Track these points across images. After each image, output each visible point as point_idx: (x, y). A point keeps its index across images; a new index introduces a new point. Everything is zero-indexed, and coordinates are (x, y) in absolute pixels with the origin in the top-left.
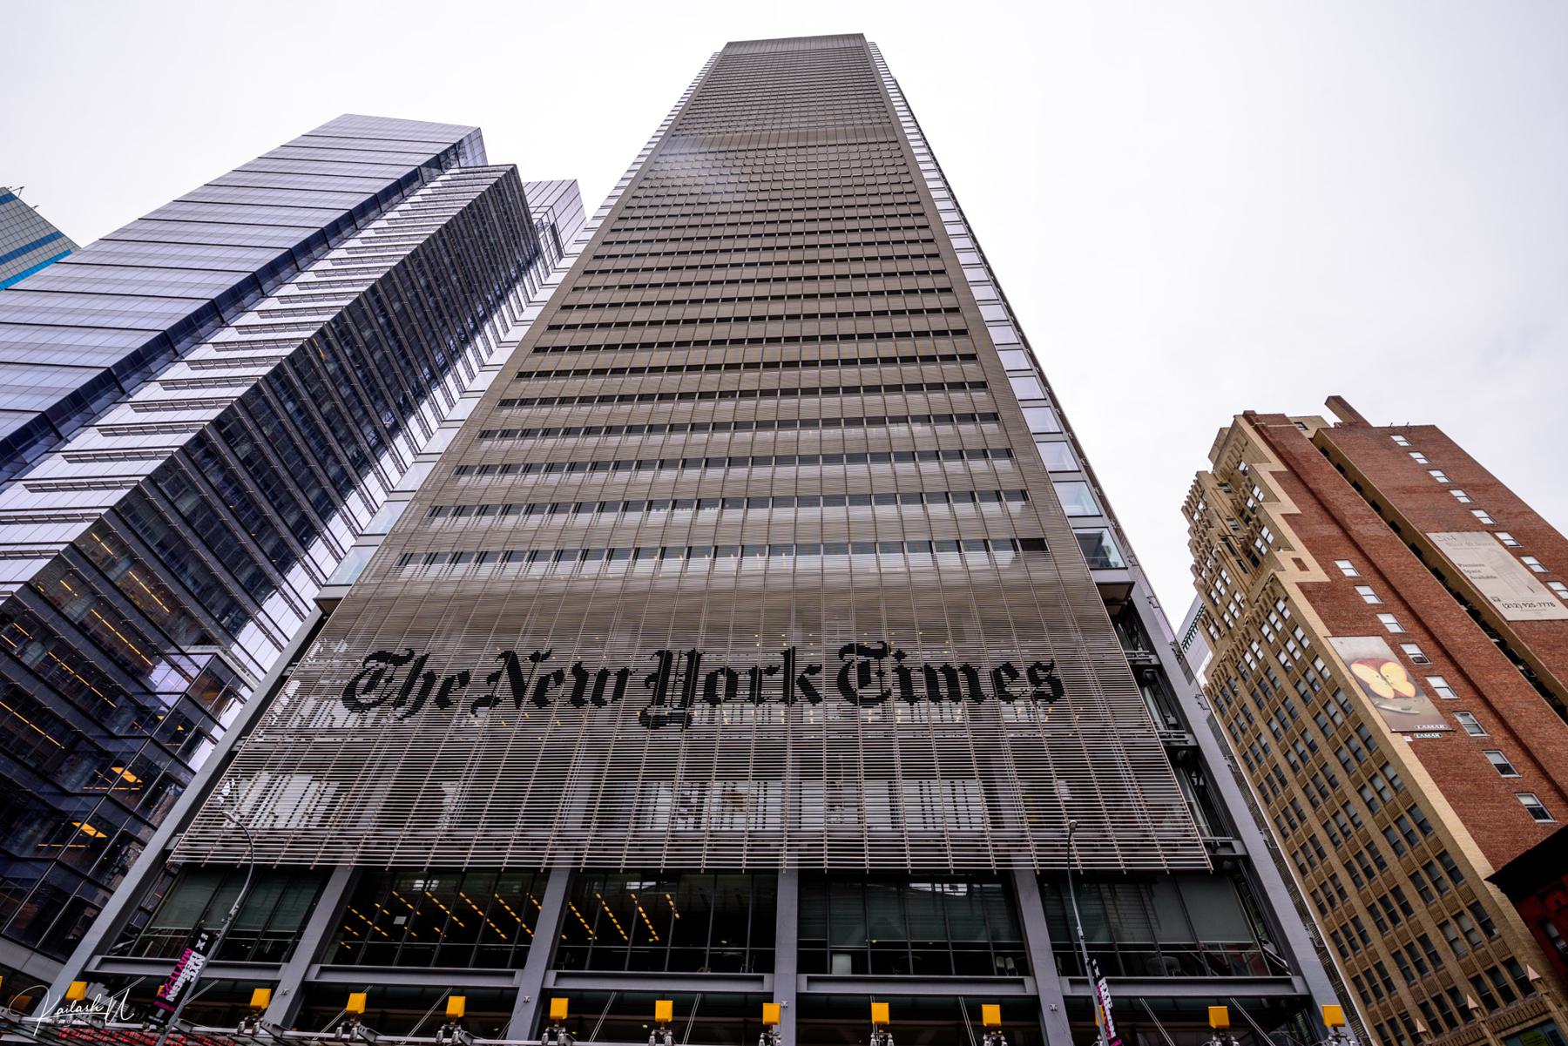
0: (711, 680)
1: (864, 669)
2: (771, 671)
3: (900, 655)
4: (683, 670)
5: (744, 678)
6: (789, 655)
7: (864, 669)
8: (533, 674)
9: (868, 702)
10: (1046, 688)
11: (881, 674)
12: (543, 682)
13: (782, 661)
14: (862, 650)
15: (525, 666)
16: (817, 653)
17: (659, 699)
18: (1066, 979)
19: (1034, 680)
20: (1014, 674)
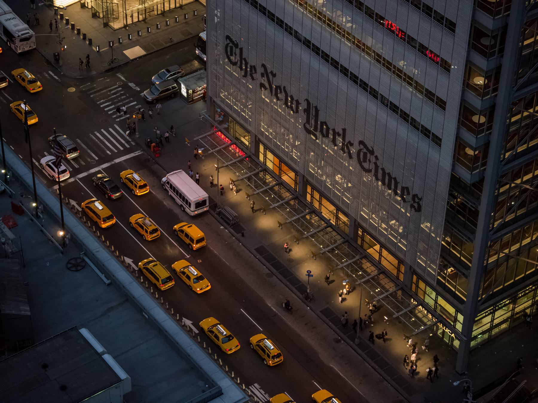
0: (322, 123)
1: (365, 155)
3: (376, 158)
4: (314, 115)
7: (365, 155)
10: (416, 205)
11: (370, 161)
13: (341, 132)
16: (354, 137)
17: (308, 121)
20: (408, 193)
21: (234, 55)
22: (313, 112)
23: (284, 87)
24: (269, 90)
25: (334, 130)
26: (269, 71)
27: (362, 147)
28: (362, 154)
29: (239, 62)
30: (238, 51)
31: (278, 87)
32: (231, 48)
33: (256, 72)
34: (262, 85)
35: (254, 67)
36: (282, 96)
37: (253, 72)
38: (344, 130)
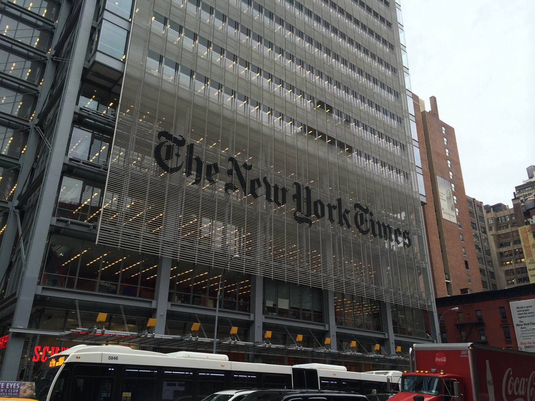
0: (316, 203)
2: (335, 207)
3: (371, 214)
4: (305, 197)
5: (326, 209)
6: (339, 200)
7: (361, 215)
8: (248, 176)
9: (364, 233)
11: (366, 221)
12: (253, 182)
14: (361, 208)
15: (243, 170)
16: (349, 202)
17: (299, 209)
18: (264, 316)
19: (404, 237)
21: (175, 157)
22: (304, 194)
23: (265, 179)
25: (329, 205)
26: (240, 164)
27: (358, 209)
28: (359, 216)
33: (217, 170)
36: (261, 191)
38: (339, 200)
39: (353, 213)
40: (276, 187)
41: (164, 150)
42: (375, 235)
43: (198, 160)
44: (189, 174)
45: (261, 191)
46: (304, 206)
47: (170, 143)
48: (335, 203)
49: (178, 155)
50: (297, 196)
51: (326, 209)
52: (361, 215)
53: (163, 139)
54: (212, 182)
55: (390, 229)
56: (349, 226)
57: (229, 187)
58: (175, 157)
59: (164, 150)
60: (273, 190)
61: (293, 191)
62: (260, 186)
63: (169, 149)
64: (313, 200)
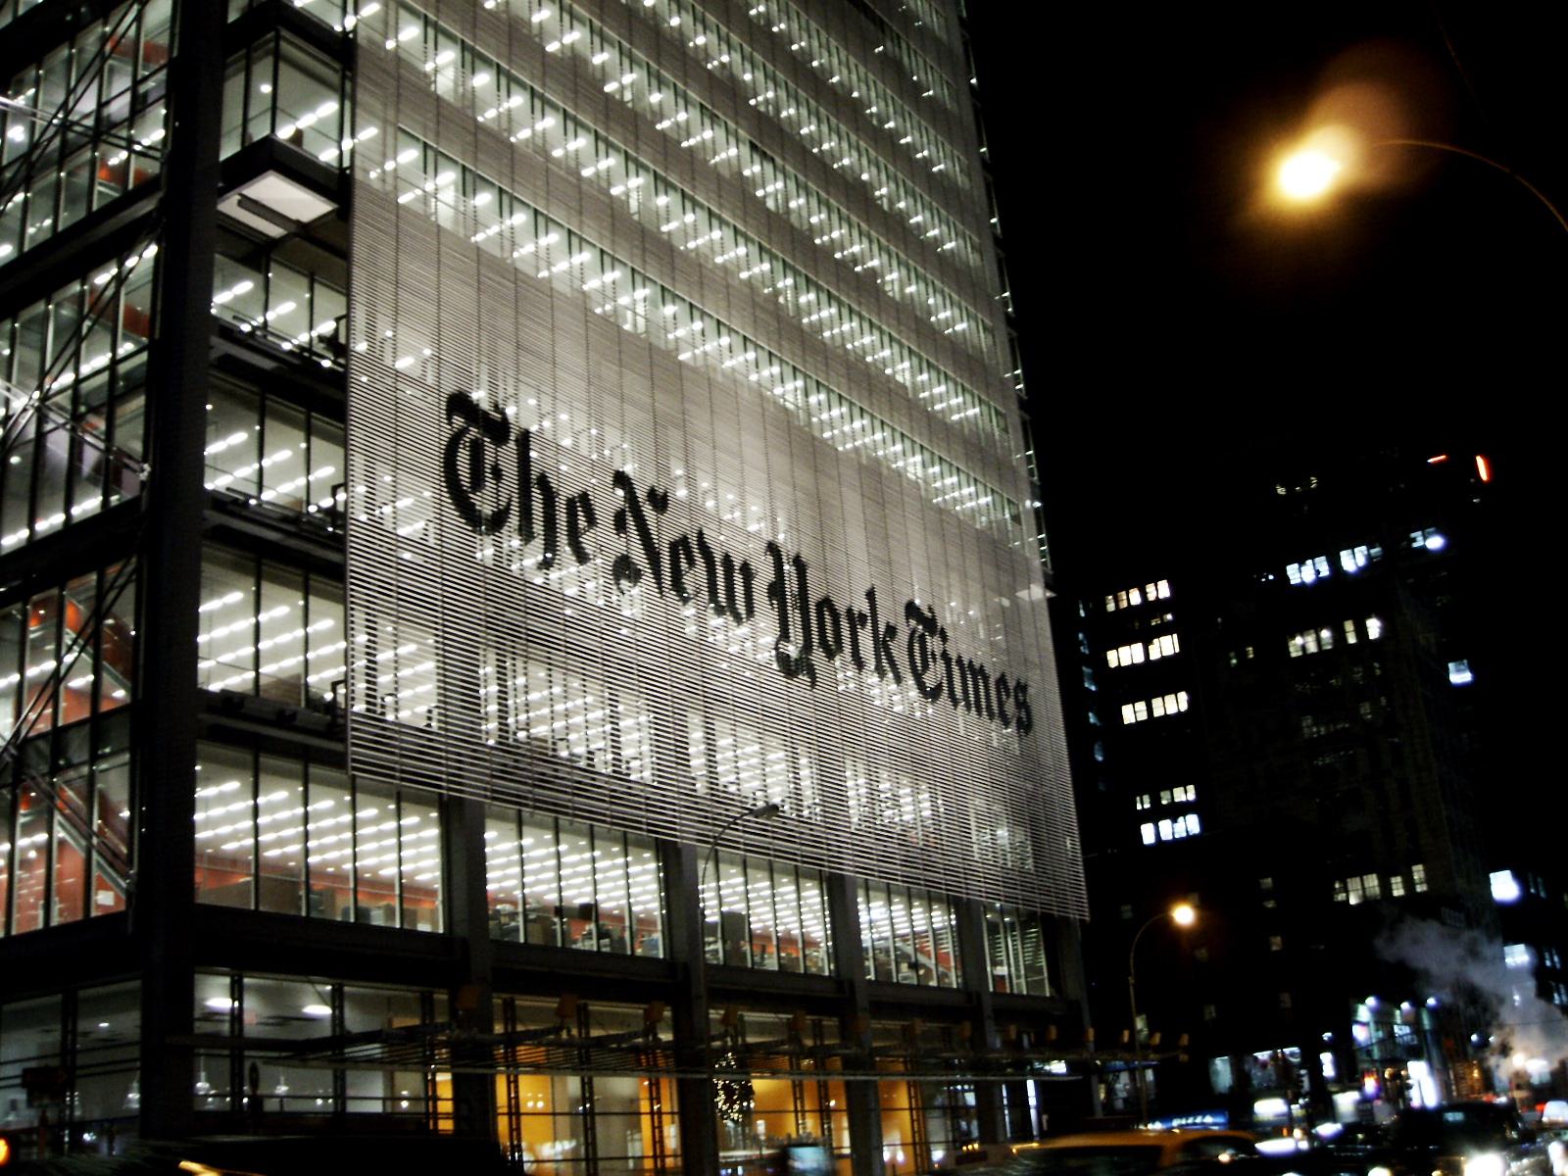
2: (862, 618)
3: (944, 638)
4: (796, 590)
5: (845, 624)
9: (933, 694)
10: (1023, 715)
13: (865, 608)
17: (784, 635)
24: (648, 577)
27: (913, 622)
29: (515, 508)
30: (507, 456)
31: (680, 546)
32: (477, 450)
33: (592, 521)
34: (624, 569)
35: (584, 497)
36: (695, 577)
37: (582, 523)
38: (871, 595)
39: (903, 636)
40: (727, 561)
41: (463, 458)
42: (955, 702)
43: (543, 482)
44: (527, 534)
45: (695, 577)
46: (795, 617)
47: (474, 432)
48: (862, 606)
49: (497, 473)
50: (776, 590)
51: (845, 624)
52: (922, 638)
53: (459, 421)
54: (582, 557)
55: (986, 678)
56: (898, 679)
57: (624, 569)
58: (490, 483)
59: (463, 458)
60: (720, 571)
61: (764, 574)
62: (691, 562)
63: (477, 450)
64: (814, 597)
